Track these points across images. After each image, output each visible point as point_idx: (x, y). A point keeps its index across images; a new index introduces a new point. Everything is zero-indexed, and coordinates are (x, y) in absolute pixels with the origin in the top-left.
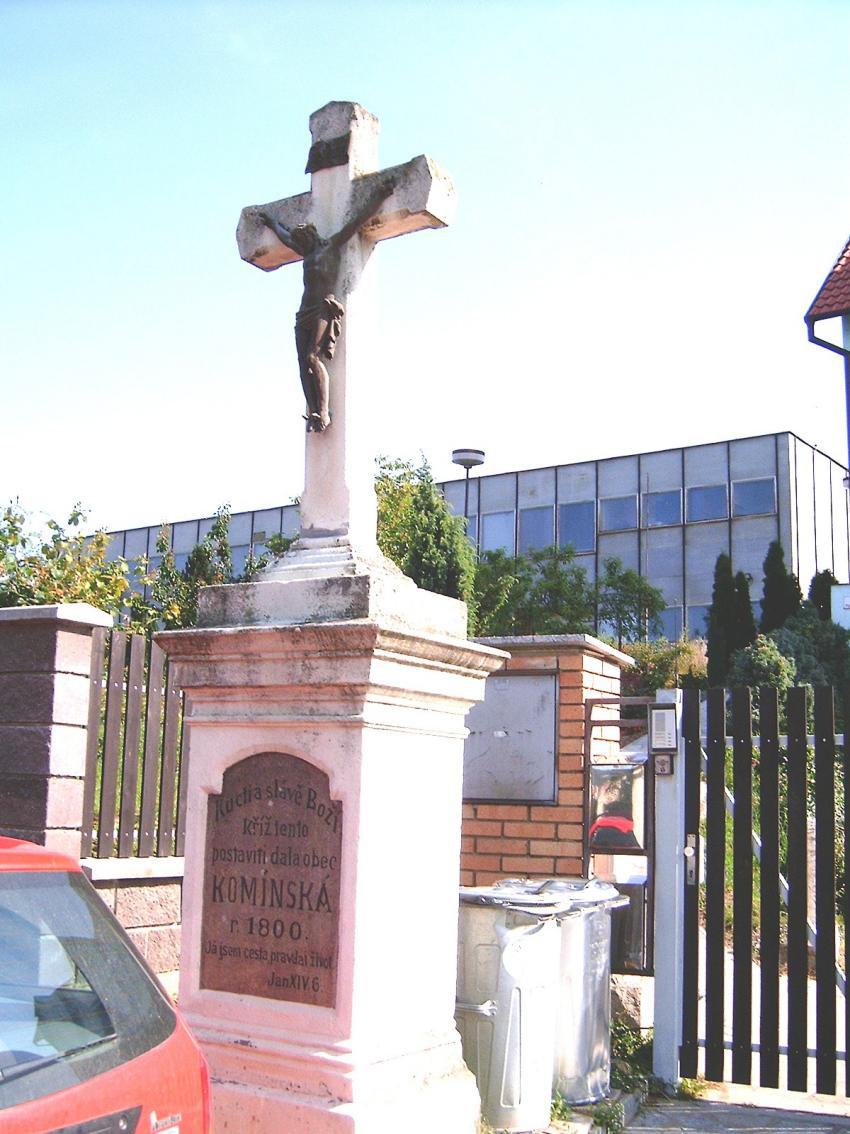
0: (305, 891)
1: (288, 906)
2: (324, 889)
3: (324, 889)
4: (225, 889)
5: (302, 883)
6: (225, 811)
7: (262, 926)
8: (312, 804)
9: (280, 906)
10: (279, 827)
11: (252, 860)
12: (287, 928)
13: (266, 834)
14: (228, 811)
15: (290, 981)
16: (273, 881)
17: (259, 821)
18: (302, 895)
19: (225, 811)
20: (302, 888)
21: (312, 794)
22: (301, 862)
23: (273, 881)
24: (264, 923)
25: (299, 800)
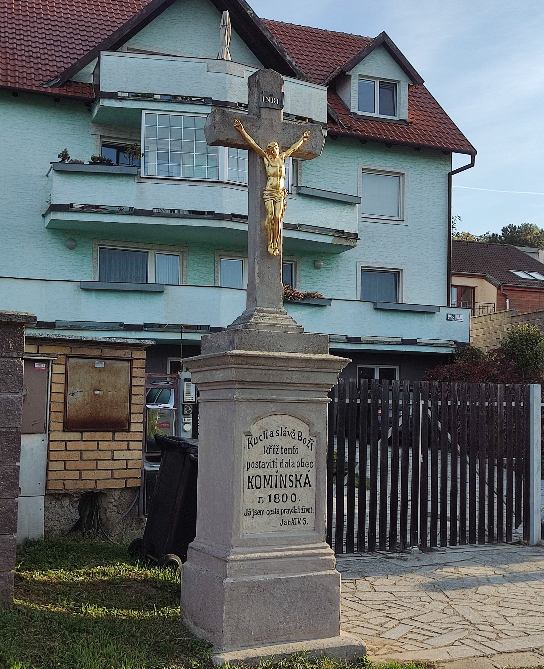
0: (298, 479)
1: (289, 486)
2: (307, 475)
3: (307, 475)
4: (253, 482)
5: (296, 475)
6: (253, 443)
7: (275, 498)
8: (300, 438)
9: (285, 487)
10: (283, 450)
11: (269, 467)
12: (289, 498)
13: (277, 454)
14: (255, 444)
15: (292, 522)
16: (281, 475)
17: (272, 447)
18: (296, 481)
19: (253, 443)
20: (296, 478)
21: (300, 434)
22: (296, 465)
23: (281, 475)
24: (277, 496)
25: (293, 437)
